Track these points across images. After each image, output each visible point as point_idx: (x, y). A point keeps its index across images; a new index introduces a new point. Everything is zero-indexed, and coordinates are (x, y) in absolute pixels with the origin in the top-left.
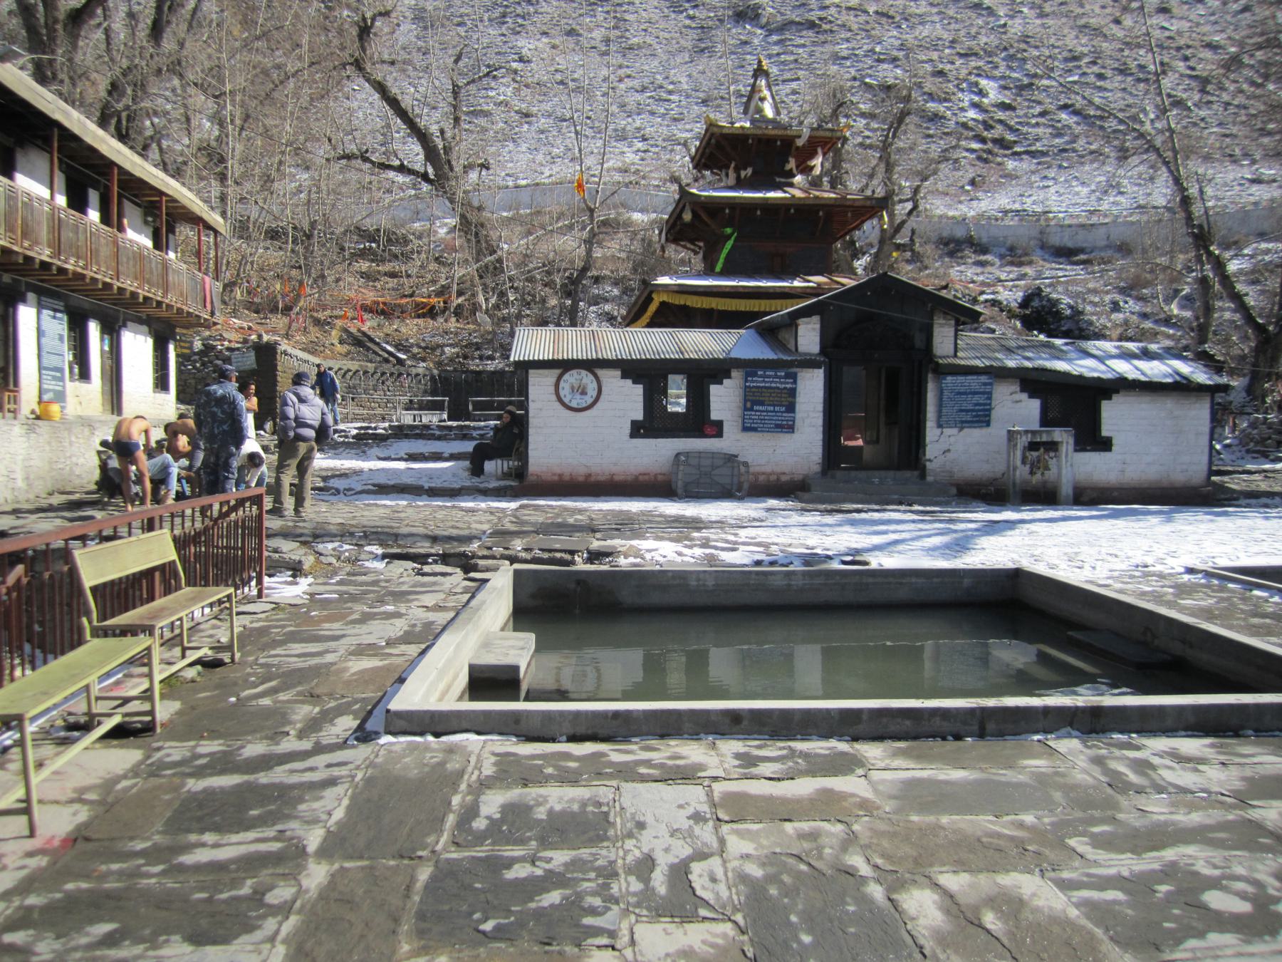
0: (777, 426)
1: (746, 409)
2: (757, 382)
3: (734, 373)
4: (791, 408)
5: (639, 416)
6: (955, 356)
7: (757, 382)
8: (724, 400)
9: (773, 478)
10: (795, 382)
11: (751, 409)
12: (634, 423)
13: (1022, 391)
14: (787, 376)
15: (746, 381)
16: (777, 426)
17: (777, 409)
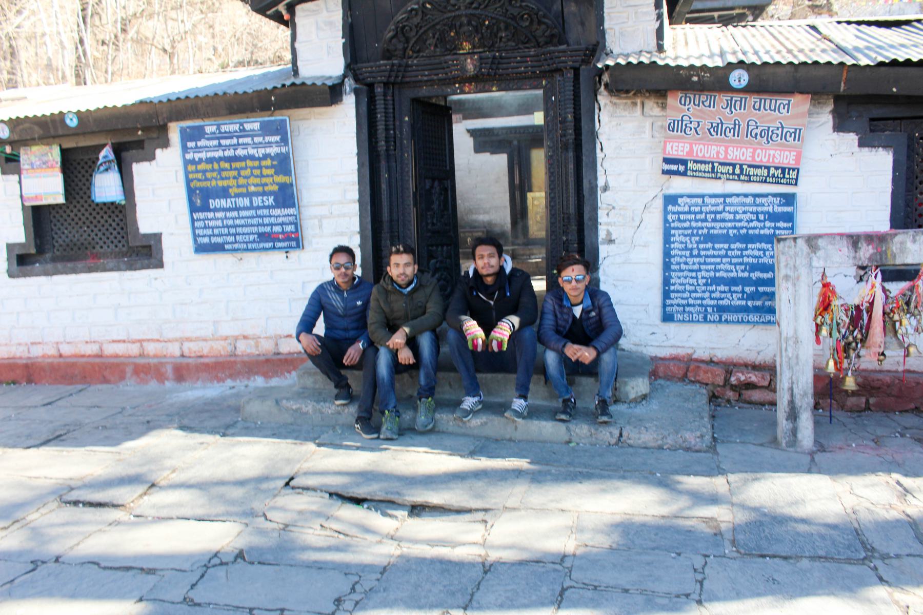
0: (263, 237)
1: (193, 209)
2: (207, 149)
3: (175, 131)
4: (286, 197)
5: (18, 233)
6: (660, 48)
7: (207, 149)
8: (159, 191)
9: (267, 347)
10: (284, 141)
11: (206, 208)
12: (10, 247)
13: (839, 127)
14: (266, 129)
15: (185, 149)
16: (263, 237)
17: (257, 201)
